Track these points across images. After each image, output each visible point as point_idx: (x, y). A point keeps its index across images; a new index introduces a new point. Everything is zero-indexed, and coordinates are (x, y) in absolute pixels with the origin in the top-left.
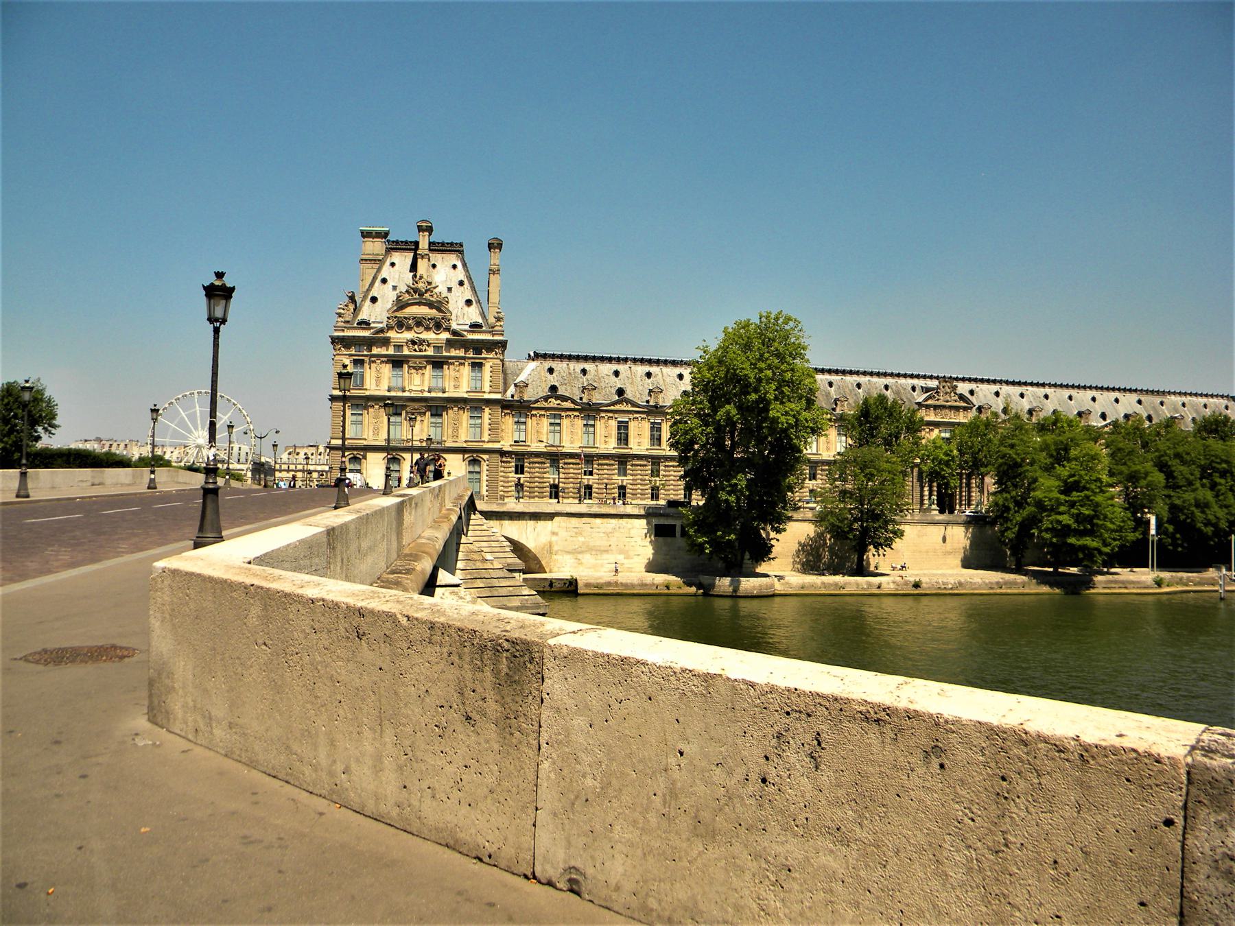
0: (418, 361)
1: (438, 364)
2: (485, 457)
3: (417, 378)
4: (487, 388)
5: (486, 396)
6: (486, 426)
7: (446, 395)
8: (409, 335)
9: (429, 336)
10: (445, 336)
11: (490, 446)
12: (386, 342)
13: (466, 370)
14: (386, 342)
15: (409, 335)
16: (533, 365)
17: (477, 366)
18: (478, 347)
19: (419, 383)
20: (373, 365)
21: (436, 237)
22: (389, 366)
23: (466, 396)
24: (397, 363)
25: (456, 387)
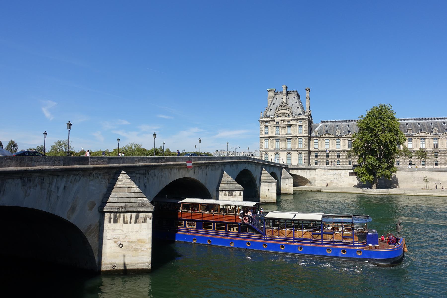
1: (289, 126)
2: (304, 152)
3: (283, 131)
4: (304, 133)
5: (303, 135)
9: (286, 118)
10: (291, 118)
14: (275, 121)
19: (282, 132)
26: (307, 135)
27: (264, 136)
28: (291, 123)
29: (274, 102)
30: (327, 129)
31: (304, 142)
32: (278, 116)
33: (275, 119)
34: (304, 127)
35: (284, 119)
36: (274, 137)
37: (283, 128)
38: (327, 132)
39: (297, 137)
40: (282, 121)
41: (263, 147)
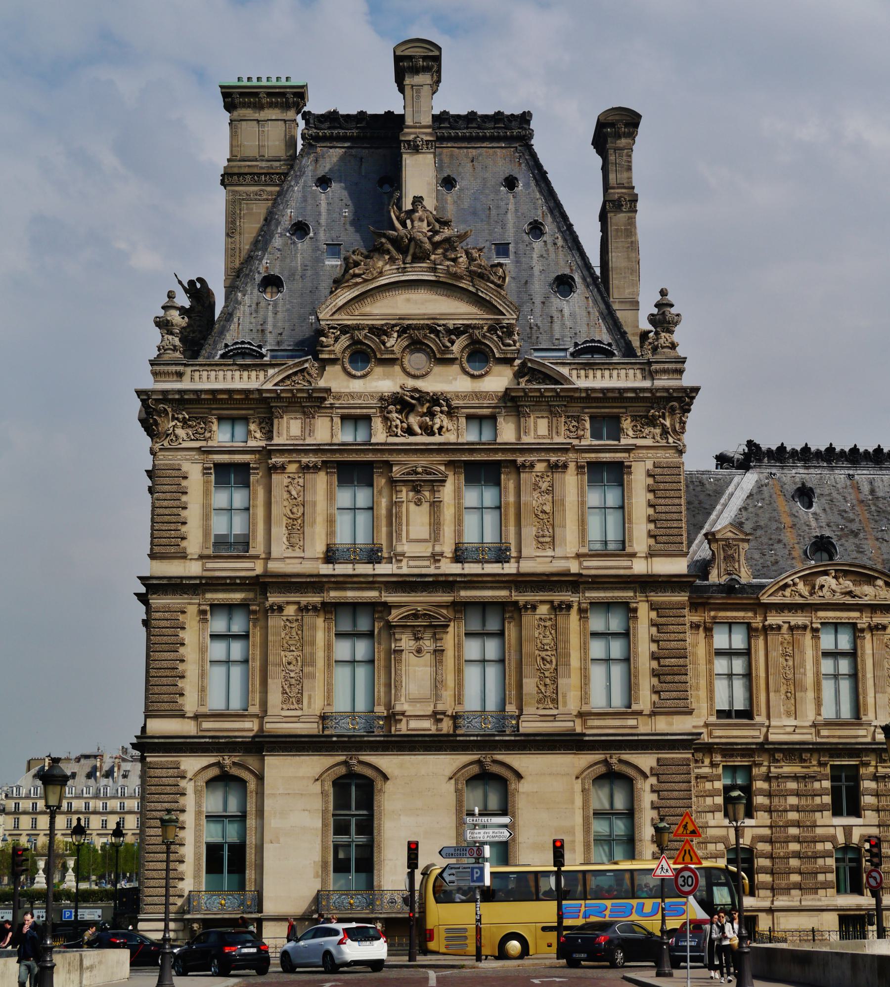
0: (421, 461)
1: (483, 470)
2: (646, 761)
4: (640, 542)
5: (639, 567)
6: (644, 663)
7: (510, 568)
8: (384, 382)
9: (449, 382)
10: (498, 381)
11: (663, 725)
12: (313, 403)
13: (571, 482)
15: (384, 382)
16: (748, 481)
17: (611, 473)
18: (607, 411)
20: (278, 479)
21: (454, 97)
22: (321, 480)
23: (574, 568)
24: (352, 469)
25: (548, 539)
26: (678, 566)
27: (194, 569)
28: (507, 432)
29: (289, 214)
30: (814, 520)
31: (644, 647)
32: (363, 355)
33: (334, 380)
34: (638, 479)
35: (429, 386)
36: (316, 583)
37: (423, 484)
38: (822, 546)
39: (576, 582)
40: (402, 403)
41: (190, 704)
